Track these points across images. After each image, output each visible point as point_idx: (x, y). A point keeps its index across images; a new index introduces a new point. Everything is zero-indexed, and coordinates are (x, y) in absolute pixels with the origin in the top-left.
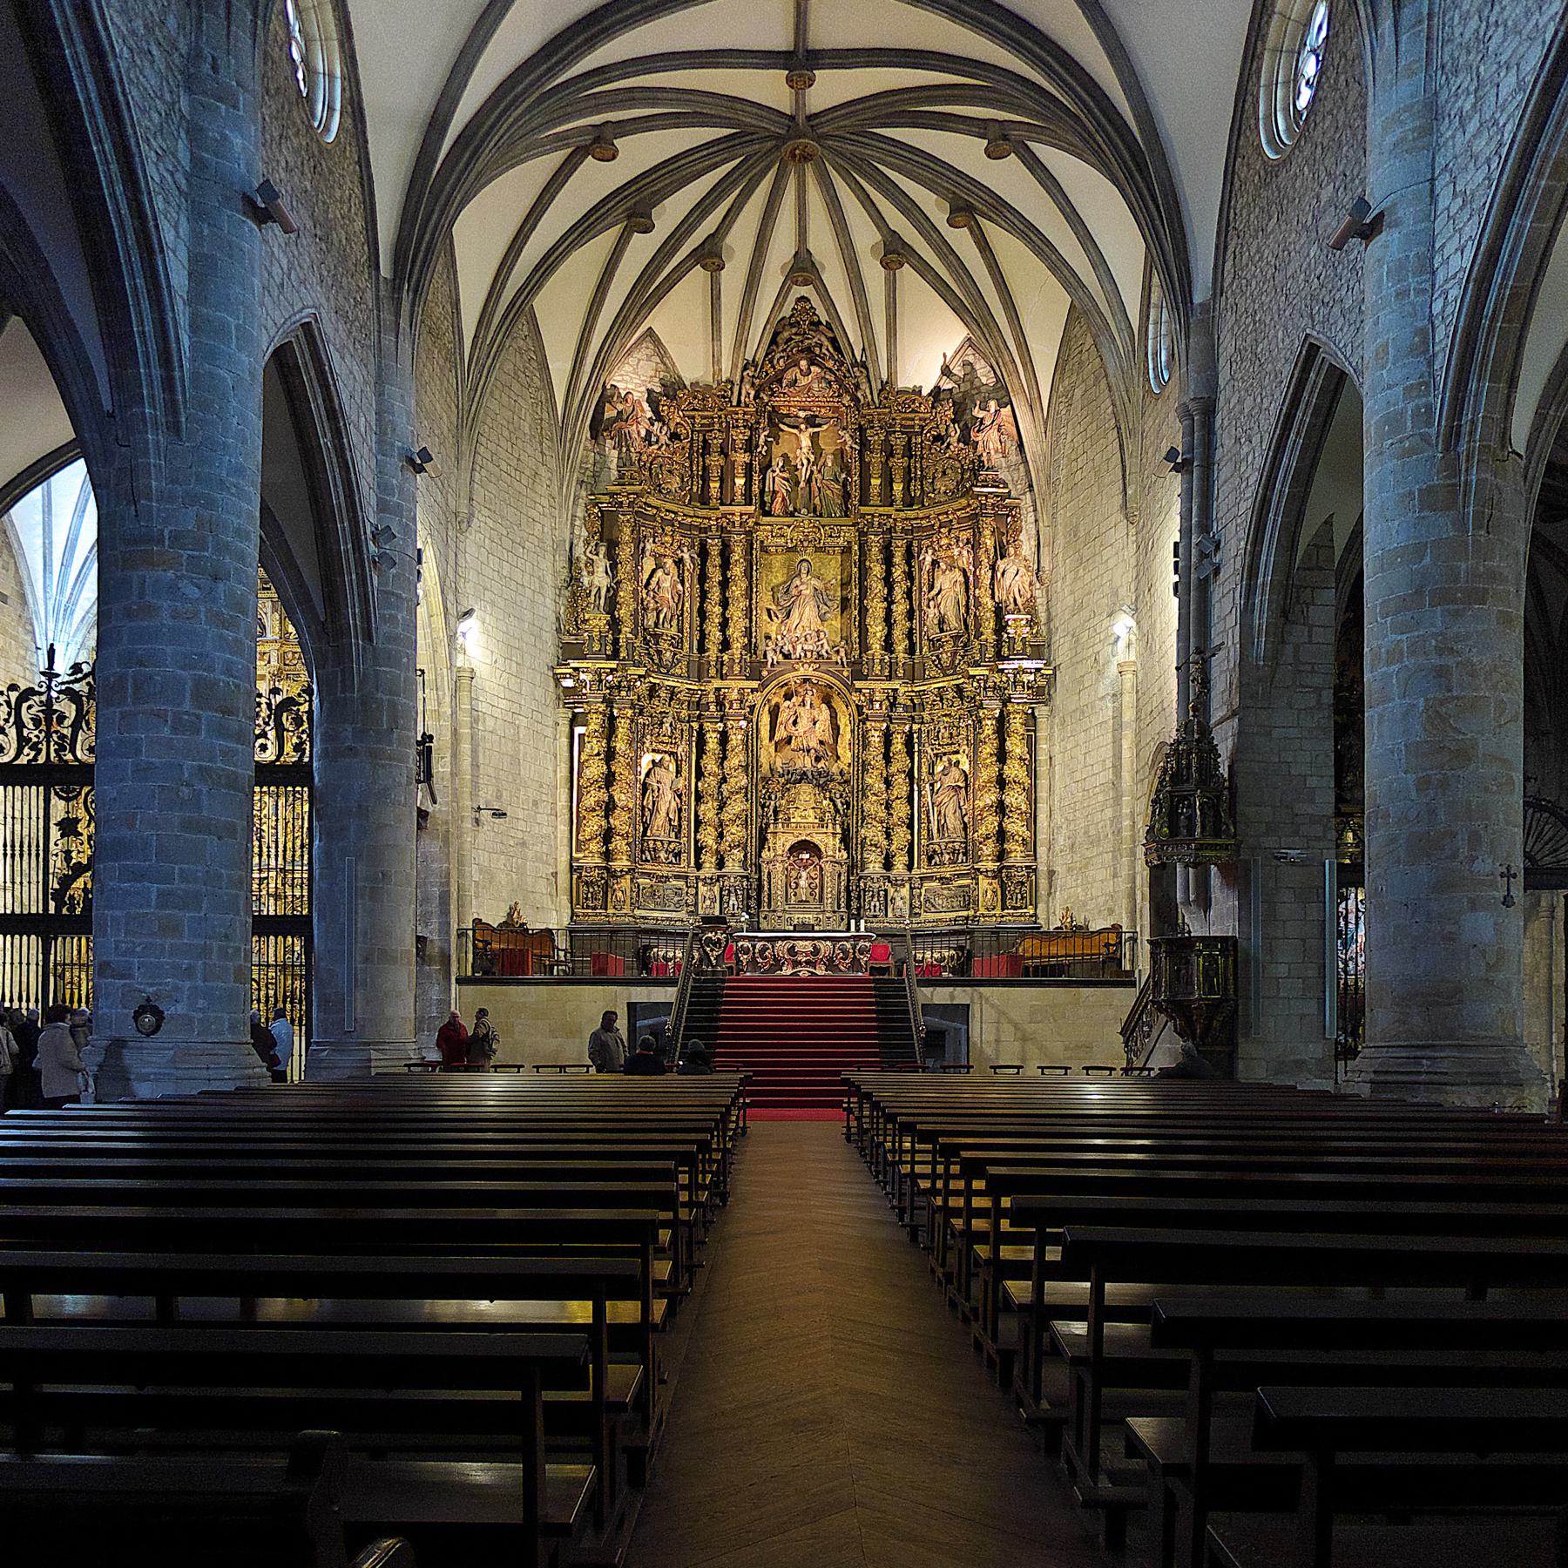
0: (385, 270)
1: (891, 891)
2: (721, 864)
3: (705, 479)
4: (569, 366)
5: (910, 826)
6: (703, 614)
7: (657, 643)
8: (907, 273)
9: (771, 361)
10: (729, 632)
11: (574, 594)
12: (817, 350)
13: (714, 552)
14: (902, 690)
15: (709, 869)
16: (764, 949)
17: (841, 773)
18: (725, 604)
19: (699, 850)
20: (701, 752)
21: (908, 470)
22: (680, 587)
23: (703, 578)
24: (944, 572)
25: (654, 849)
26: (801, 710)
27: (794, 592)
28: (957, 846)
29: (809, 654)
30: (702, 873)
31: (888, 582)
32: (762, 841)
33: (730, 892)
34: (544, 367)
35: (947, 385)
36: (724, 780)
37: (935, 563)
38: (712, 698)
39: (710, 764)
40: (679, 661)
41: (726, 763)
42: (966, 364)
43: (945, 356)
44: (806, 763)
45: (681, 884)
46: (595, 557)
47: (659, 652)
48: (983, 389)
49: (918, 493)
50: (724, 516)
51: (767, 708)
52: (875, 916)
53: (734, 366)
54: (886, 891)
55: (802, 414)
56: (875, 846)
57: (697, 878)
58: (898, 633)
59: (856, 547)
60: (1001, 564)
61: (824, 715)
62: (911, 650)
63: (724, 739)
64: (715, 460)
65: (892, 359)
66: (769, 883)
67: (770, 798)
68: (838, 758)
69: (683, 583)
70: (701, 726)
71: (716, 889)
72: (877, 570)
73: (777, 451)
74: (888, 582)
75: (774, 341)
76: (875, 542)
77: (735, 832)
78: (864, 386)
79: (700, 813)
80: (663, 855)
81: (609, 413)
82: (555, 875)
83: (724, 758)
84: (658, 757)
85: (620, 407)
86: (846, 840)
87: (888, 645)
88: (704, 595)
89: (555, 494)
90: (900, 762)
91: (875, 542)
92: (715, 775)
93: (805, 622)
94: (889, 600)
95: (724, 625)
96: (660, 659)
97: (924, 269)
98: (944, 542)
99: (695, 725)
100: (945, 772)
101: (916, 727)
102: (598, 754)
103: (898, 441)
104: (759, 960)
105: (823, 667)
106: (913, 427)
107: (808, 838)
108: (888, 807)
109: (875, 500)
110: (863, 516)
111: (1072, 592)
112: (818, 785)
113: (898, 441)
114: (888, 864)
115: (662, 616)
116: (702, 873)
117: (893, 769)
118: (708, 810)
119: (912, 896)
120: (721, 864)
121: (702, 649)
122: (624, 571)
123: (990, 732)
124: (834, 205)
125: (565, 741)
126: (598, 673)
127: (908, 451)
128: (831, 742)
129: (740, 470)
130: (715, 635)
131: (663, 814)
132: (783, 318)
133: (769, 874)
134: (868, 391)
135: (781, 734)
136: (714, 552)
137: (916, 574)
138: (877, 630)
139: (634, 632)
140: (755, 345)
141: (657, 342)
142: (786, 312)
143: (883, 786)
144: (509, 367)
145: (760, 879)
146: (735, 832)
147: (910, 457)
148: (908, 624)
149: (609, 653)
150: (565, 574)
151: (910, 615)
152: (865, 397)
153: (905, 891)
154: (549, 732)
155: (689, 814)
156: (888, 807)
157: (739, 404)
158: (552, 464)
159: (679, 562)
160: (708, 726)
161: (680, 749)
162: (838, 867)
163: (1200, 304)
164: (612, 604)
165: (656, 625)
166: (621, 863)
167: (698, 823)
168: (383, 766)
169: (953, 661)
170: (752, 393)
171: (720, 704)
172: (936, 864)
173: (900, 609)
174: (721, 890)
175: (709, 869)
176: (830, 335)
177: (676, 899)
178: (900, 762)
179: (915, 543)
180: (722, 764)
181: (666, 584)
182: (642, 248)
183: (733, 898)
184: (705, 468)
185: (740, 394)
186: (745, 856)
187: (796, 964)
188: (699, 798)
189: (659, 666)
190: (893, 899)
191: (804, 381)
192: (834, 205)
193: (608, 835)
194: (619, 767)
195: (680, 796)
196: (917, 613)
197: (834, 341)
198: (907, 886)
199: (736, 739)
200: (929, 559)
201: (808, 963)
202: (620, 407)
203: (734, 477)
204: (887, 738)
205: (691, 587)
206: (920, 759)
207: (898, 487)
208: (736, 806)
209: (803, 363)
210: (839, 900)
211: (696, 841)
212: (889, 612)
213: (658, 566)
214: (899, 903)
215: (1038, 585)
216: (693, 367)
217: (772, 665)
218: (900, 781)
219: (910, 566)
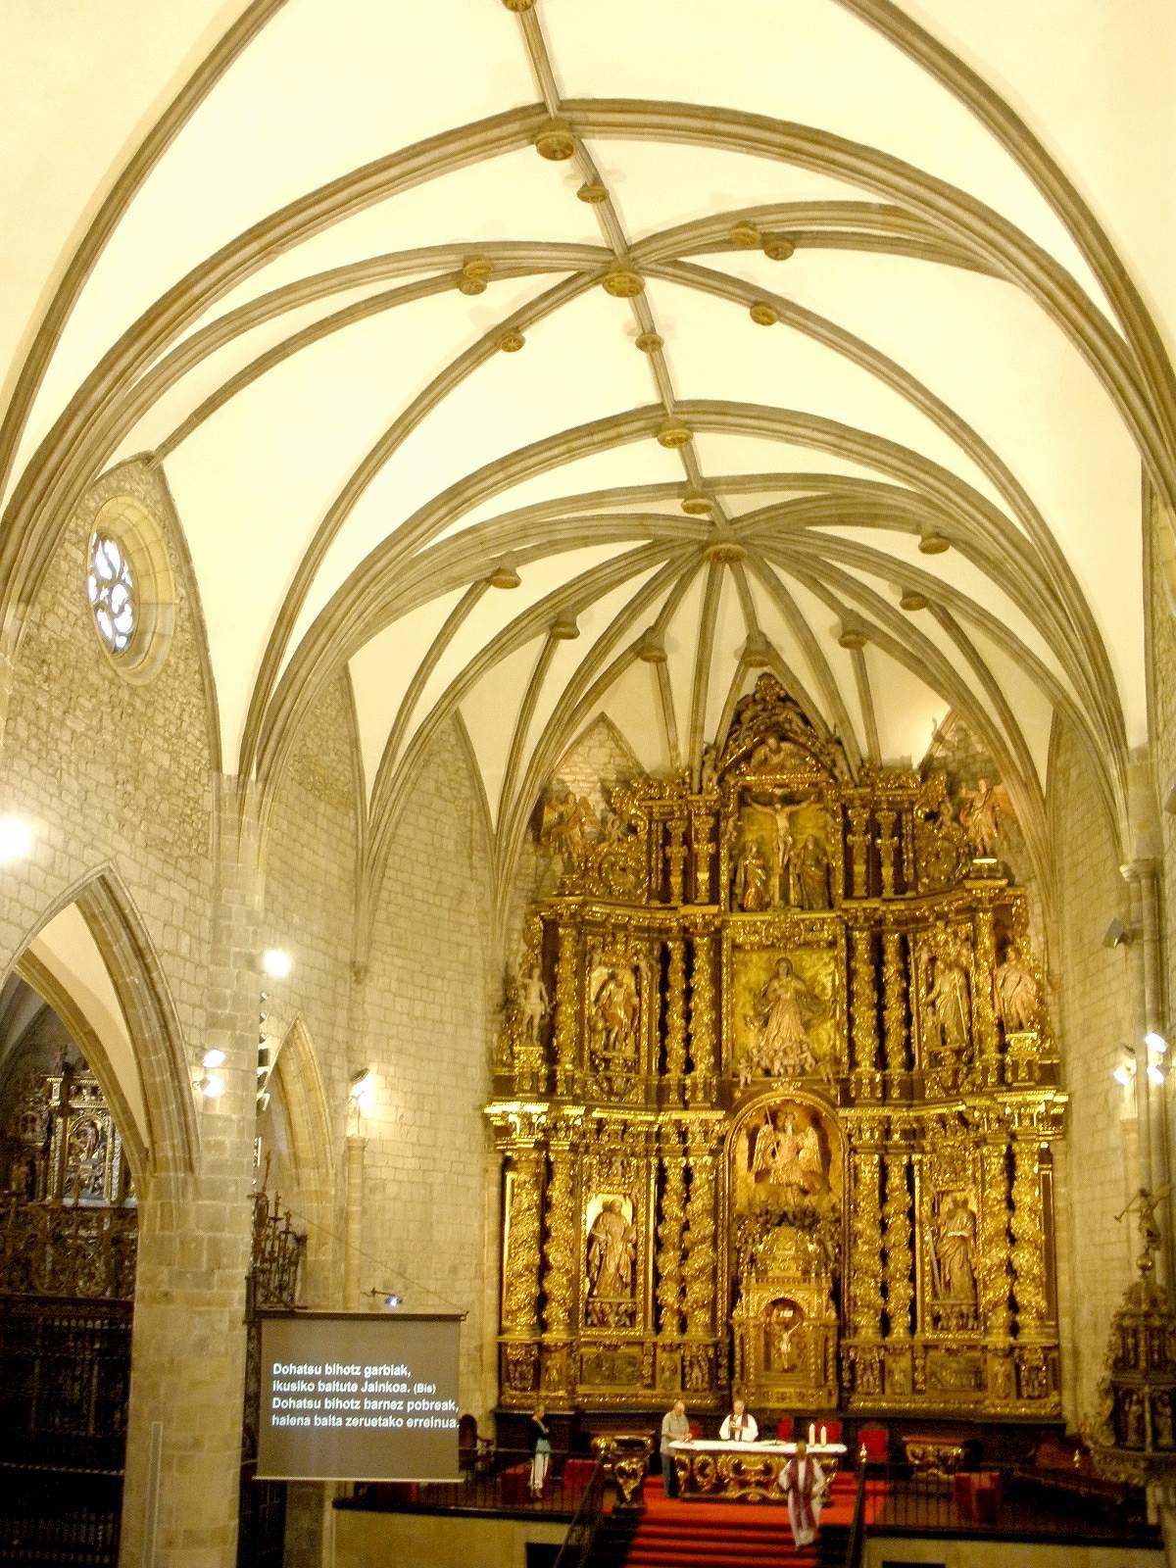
0: (230, 764)
1: (889, 1361)
2: (683, 1327)
3: (666, 873)
4: (502, 771)
5: (912, 1278)
6: (664, 1028)
7: (607, 1068)
8: (872, 650)
10: (692, 1051)
11: (509, 1019)
12: (787, 726)
13: (677, 956)
15: (671, 1333)
16: (705, 1465)
17: (834, 1209)
18: (687, 1016)
19: (658, 1309)
20: (662, 1191)
21: (899, 852)
22: (635, 1000)
23: (664, 986)
24: (943, 972)
25: (602, 1312)
26: (781, 1136)
27: (771, 996)
29: (790, 1070)
30: (660, 1340)
31: (879, 986)
32: (735, 1296)
33: (691, 1364)
34: (474, 775)
35: (940, 753)
36: (686, 1227)
37: (933, 960)
39: (672, 1206)
40: (634, 1086)
41: (689, 1207)
42: (960, 729)
43: (934, 721)
44: (791, 1200)
45: (635, 1350)
46: (528, 981)
47: (609, 1080)
48: (979, 757)
49: (911, 878)
50: (685, 917)
51: (744, 1132)
52: (868, 1394)
53: (692, 752)
55: (778, 792)
58: (893, 1044)
59: (843, 941)
60: (1000, 973)
61: (810, 1140)
62: (909, 1063)
63: (688, 1176)
64: (677, 851)
65: (872, 731)
66: (742, 1349)
67: (746, 1242)
68: (830, 1189)
69: (639, 994)
70: (661, 1161)
73: (750, 837)
74: (879, 986)
75: (737, 720)
77: (698, 1290)
78: (841, 763)
79: (660, 1265)
80: (612, 1319)
81: (549, 816)
82: (480, 1348)
83: (688, 1199)
85: (562, 808)
86: (836, 1295)
87: (881, 1061)
88: (665, 1006)
89: (488, 906)
90: (898, 1200)
92: (677, 1219)
93: (784, 1033)
94: (880, 1007)
95: (687, 1041)
96: (611, 1088)
97: (888, 645)
98: (941, 937)
99: (654, 1161)
101: (916, 1157)
102: (529, 1209)
103: (885, 817)
104: (699, 1479)
105: (808, 1086)
107: (787, 1296)
108: (884, 1256)
109: (860, 891)
110: (846, 910)
111: (1082, 1008)
112: (803, 1227)
113: (885, 817)
114: (885, 1325)
115: (613, 1036)
116: (660, 1340)
117: (890, 1209)
118: (669, 1263)
120: (683, 1327)
121: (663, 1069)
122: (567, 987)
124: (779, 592)
125: (494, 1190)
127: (897, 829)
128: (820, 1170)
129: (704, 863)
131: (612, 1270)
132: (746, 697)
133: (742, 1338)
134: (845, 769)
135: (758, 1164)
136: (677, 956)
138: (866, 1044)
139: (578, 1061)
140: (714, 727)
141: (611, 727)
142: (748, 688)
144: (431, 785)
145: (732, 1344)
146: (698, 1290)
147: (901, 837)
149: (542, 1090)
150: (499, 997)
151: (907, 1021)
153: (905, 1362)
154: (474, 1182)
155: (646, 1268)
156: (884, 1256)
157: (700, 791)
158: (485, 875)
159: (636, 970)
161: (636, 1190)
163: (1137, 750)
164: (549, 1030)
165: (606, 1047)
166: (556, 1335)
167: (657, 1277)
168: (200, 1313)
169: (955, 1081)
170: (715, 778)
171: (683, 1135)
172: (942, 1329)
173: (894, 1013)
174: (683, 1359)
175: (671, 1333)
177: (630, 1370)
179: (910, 938)
180: (684, 1205)
181: (618, 998)
182: (569, 656)
183: (696, 1372)
184: (667, 861)
185: (701, 781)
187: (744, 1484)
188: (659, 1244)
189: (611, 1092)
190: (891, 1372)
191: (775, 760)
192: (779, 592)
193: (542, 1301)
194: (556, 1221)
196: (914, 1019)
198: (909, 1354)
199: (699, 1179)
200: (925, 956)
201: (759, 1484)
202: (562, 808)
204: (884, 1171)
205: (650, 999)
207: (887, 872)
208: (701, 1257)
209: (772, 741)
210: (826, 1370)
211: (655, 1298)
212: (880, 1020)
213: (612, 977)
215: (1049, 990)
216: (651, 755)
217: (746, 1083)
218: (898, 1221)
219: (906, 964)
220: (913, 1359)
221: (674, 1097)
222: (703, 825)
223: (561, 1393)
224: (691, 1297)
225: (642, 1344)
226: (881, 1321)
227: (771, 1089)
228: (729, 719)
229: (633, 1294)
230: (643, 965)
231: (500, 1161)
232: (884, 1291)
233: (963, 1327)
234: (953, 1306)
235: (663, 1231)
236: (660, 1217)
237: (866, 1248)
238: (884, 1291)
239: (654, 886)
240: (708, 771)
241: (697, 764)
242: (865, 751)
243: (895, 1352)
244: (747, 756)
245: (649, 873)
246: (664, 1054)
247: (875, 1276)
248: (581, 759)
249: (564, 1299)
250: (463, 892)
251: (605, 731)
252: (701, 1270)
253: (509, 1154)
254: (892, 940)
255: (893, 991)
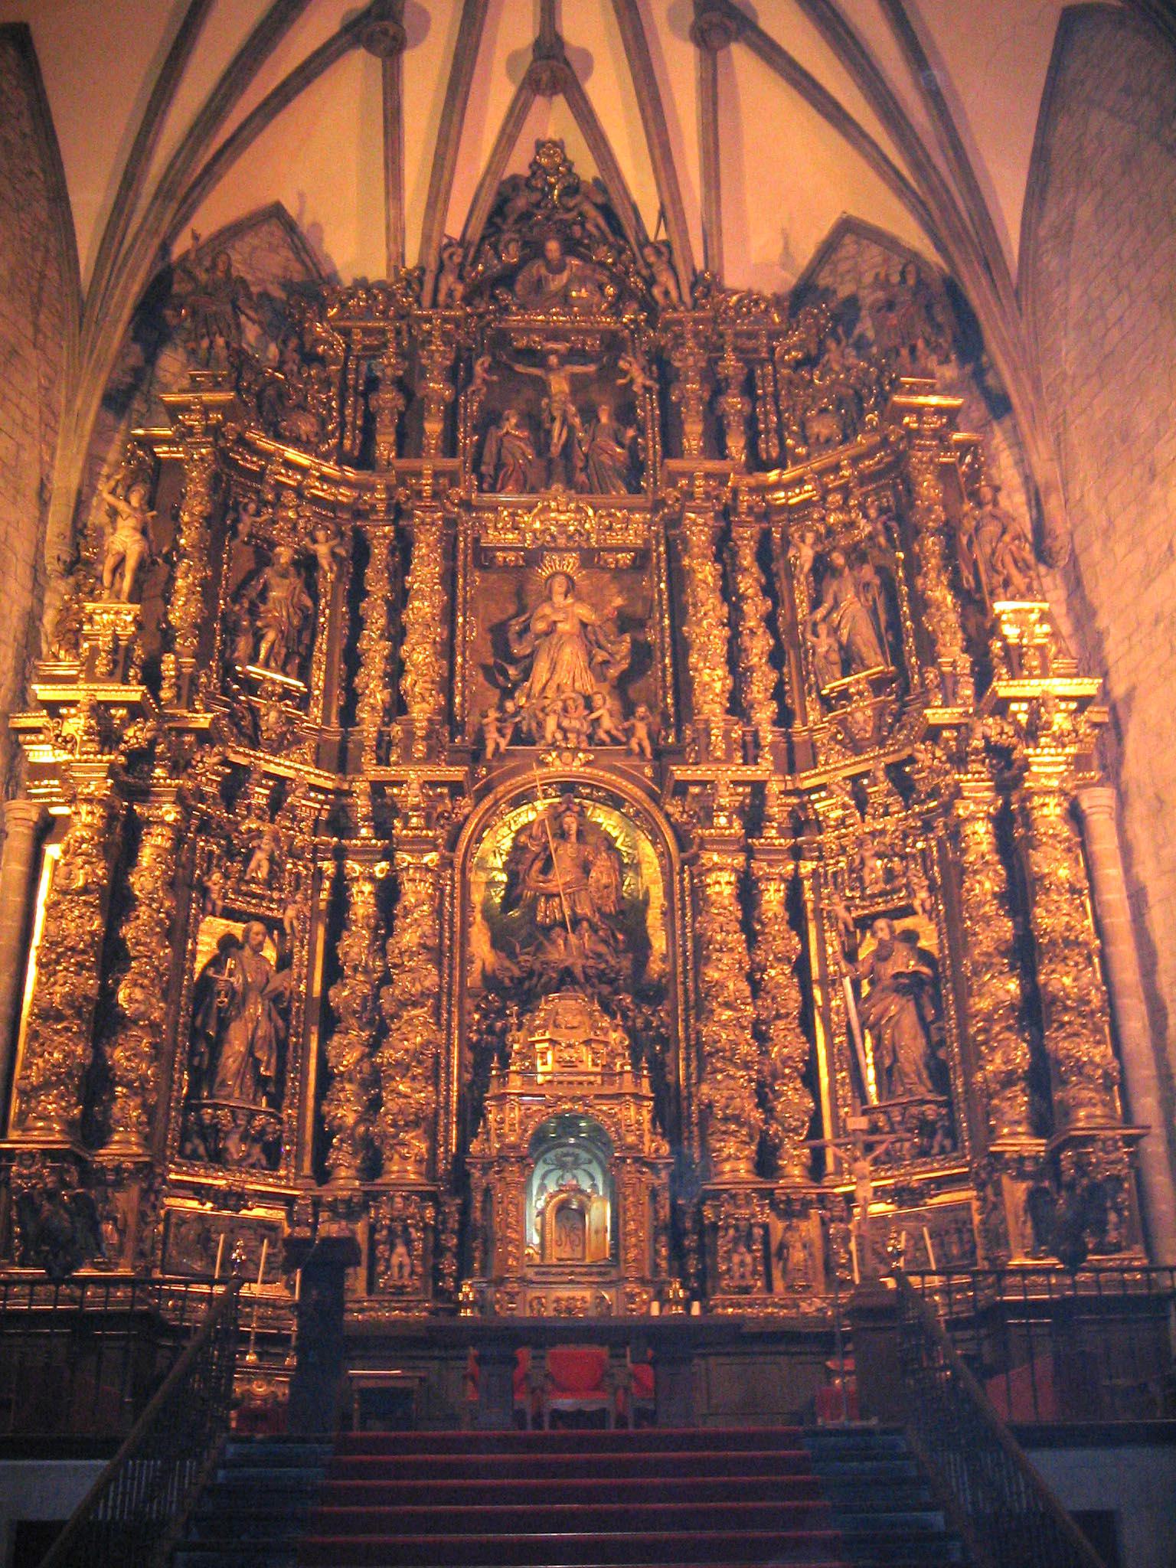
2: (372, 1167)
6: (353, 660)
8: (740, 57)
9: (495, 247)
11: (78, 588)
14: (774, 787)
15: (346, 1179)
23: (357, 593)
28: (930, 1111)
31: (728, 591)
32: (472, 1115)
34: (59, 197)
36: (387, 980)
37: (822, 569)
38: (362, 806)
52: (746, 1290)
54: (765, 1227)
56: (736, 1119)
57: (317, 1203)
63: (388, 892)
65: (711, 235)
70: (340, 868)
71: (360, 1228)
72: (706, 572)
75: (499, 210)
76: (699, 531)
78: (665, 278)
79: (331, 1053)
80: (235, 1147)
84: (238, 929)
87: (737, 706)
88: (357, 623)
90: (781, 939)
91: (699, 531)
93: (563, 677)
100: (882, 954)
102: (85, 890)
106: (756, 350)
108: (761, 1037)
114: (766, 1162)
119: (827, 1239)
120: (372, 1167)
121: (348, 716)
123: (984, 848)
126: (100, 710)
130: (376, 695)
134: (671, 285)
136: (379, 552)
137: (781, 585)
142: (519, 163)
143: (745, 987)
148: (774, 676)
151: (776, 659)
152: (666, 293)
156: (761, 1037)
157: (435, 304)
160: (353, 867)
161: (291, 912)
162: (648, 1176)
167: (326, 1077)
169: (878, 728)
170: (460, 289)
174: (373, 1229)
175: (346, 1179)
176: (599, 199)
178: (781, 939)
184: (370, 418)
185: (436, 290)
186: (432, 1150)
190: (783, 1246)
191: (557, 283)
195: (285, 1014)
197: (607, 211)
199: (415, 892)
203: (421, 419)
204: (747, 890)
206: (821, 932)
209: (553, 247)
211: (319, 1118)
214: (798, 1256)
220: (824, 1223)
221: (368, 759)
222: (438, 355)
223: (121, 1272)
224: (391, 1104)
225: (290, 1201)
226: (759, 1152)
227: (543, 764)
228: (487, 201)
229: (275, 1102)
230: (322, 550)
231: (34, 815)
232: (764, 1096)
233: (923, 1152)
234: (905, 1106)
235: (340, 995)
236: (334, 972)
237: (727, 1014)
238: (764, 1096)
239: (347, 443)
240: (449, 280)
241: (432, 265)
242: (700, 265)
243: (791, 1210)
244: (507, 278)
245: (342, 425)
246: (353, 697)
247: (747, 1066)
248: (239, 257)
249: (144, 1079)
250: (14, 352)
251: (279, 233)
252: (417, 1055)
253: (54, 811)
254: (746, 537)
255: (754, 608)
